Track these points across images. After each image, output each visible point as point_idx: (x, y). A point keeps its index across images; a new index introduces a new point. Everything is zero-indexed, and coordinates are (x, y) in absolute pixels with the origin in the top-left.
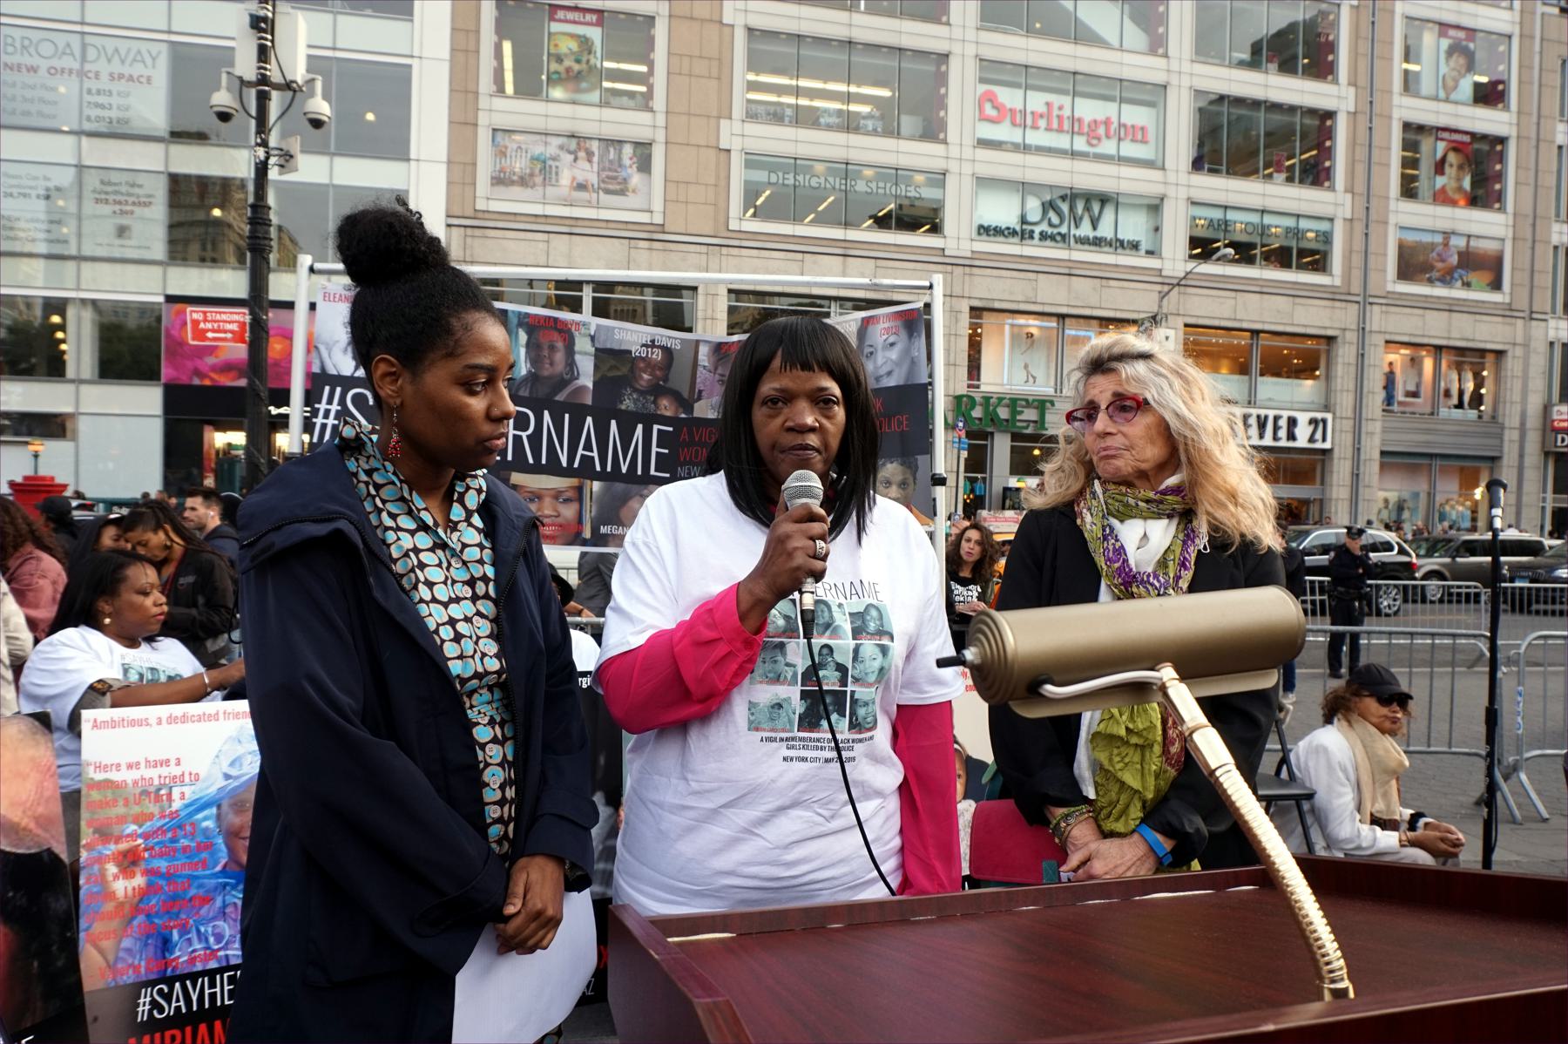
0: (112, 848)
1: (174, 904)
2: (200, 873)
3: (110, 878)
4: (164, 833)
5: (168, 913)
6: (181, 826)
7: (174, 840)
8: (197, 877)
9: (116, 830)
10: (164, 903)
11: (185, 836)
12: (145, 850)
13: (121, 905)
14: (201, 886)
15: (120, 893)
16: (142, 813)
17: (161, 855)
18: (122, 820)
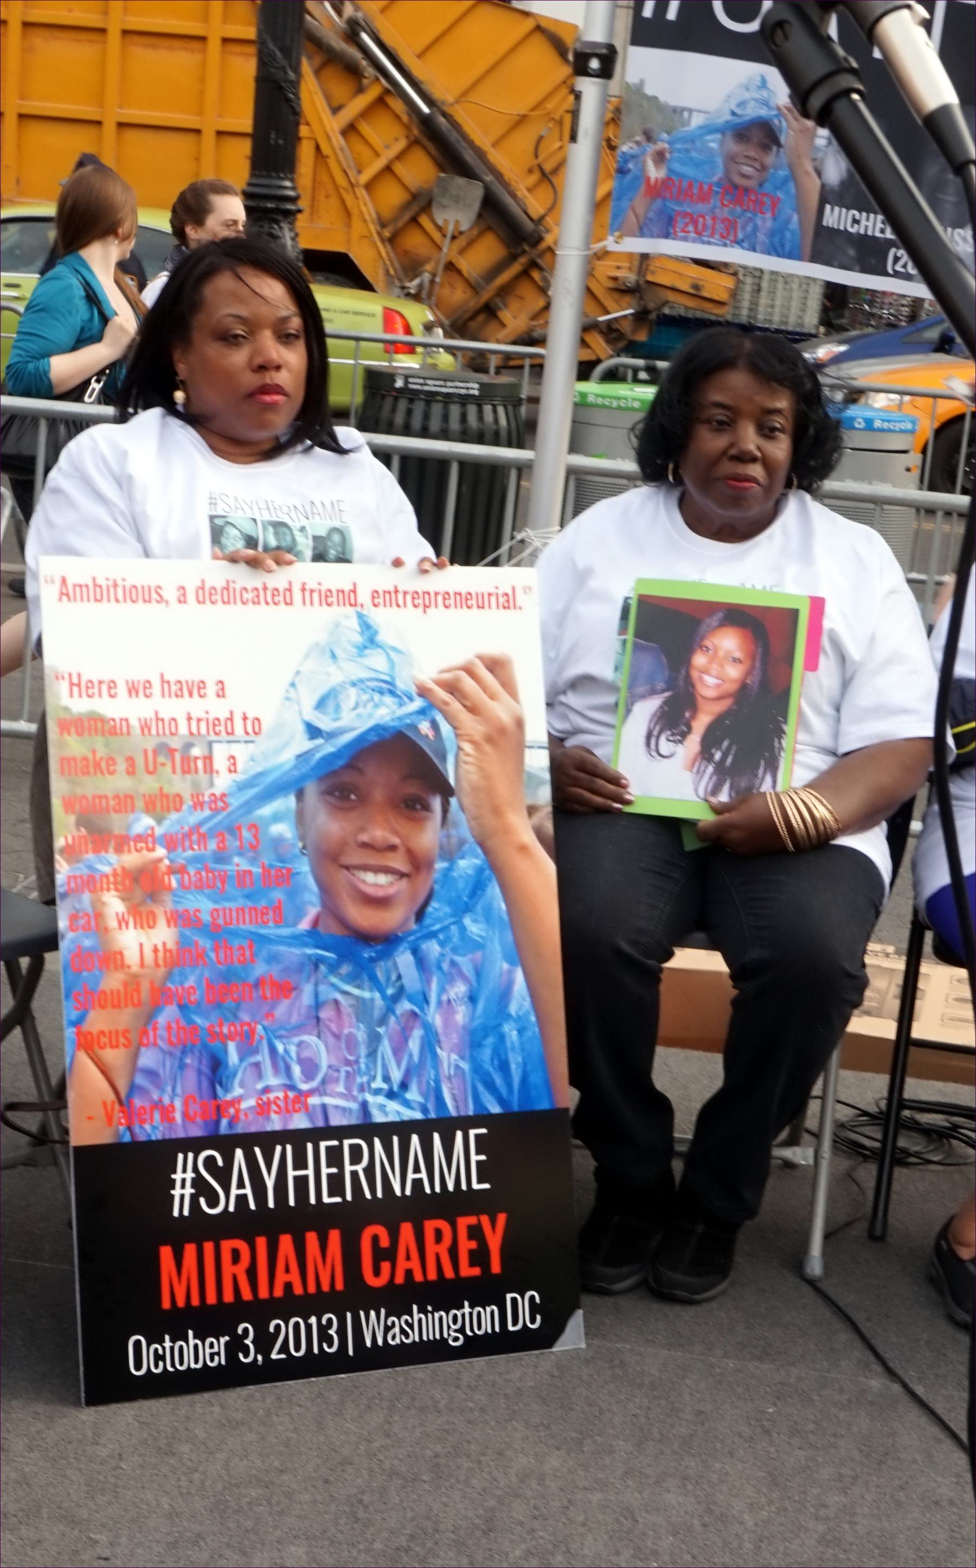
0: (109, 862)
1: (225, 991)
2: (271, 930)
3: (113, 923)
4: (203, 838)
5: (217, 1004)
6: (234, 830)
7: (221, 857)
8: (266, 939)
9: (117, 823)
10: (210, 986)
11: (241, 852)
12: (171, 871)
13: (133, 982)
14: (273, 959)
15: (132, 957)
16: (163, 795)
17: (200, 886)
18: (125, 803)
